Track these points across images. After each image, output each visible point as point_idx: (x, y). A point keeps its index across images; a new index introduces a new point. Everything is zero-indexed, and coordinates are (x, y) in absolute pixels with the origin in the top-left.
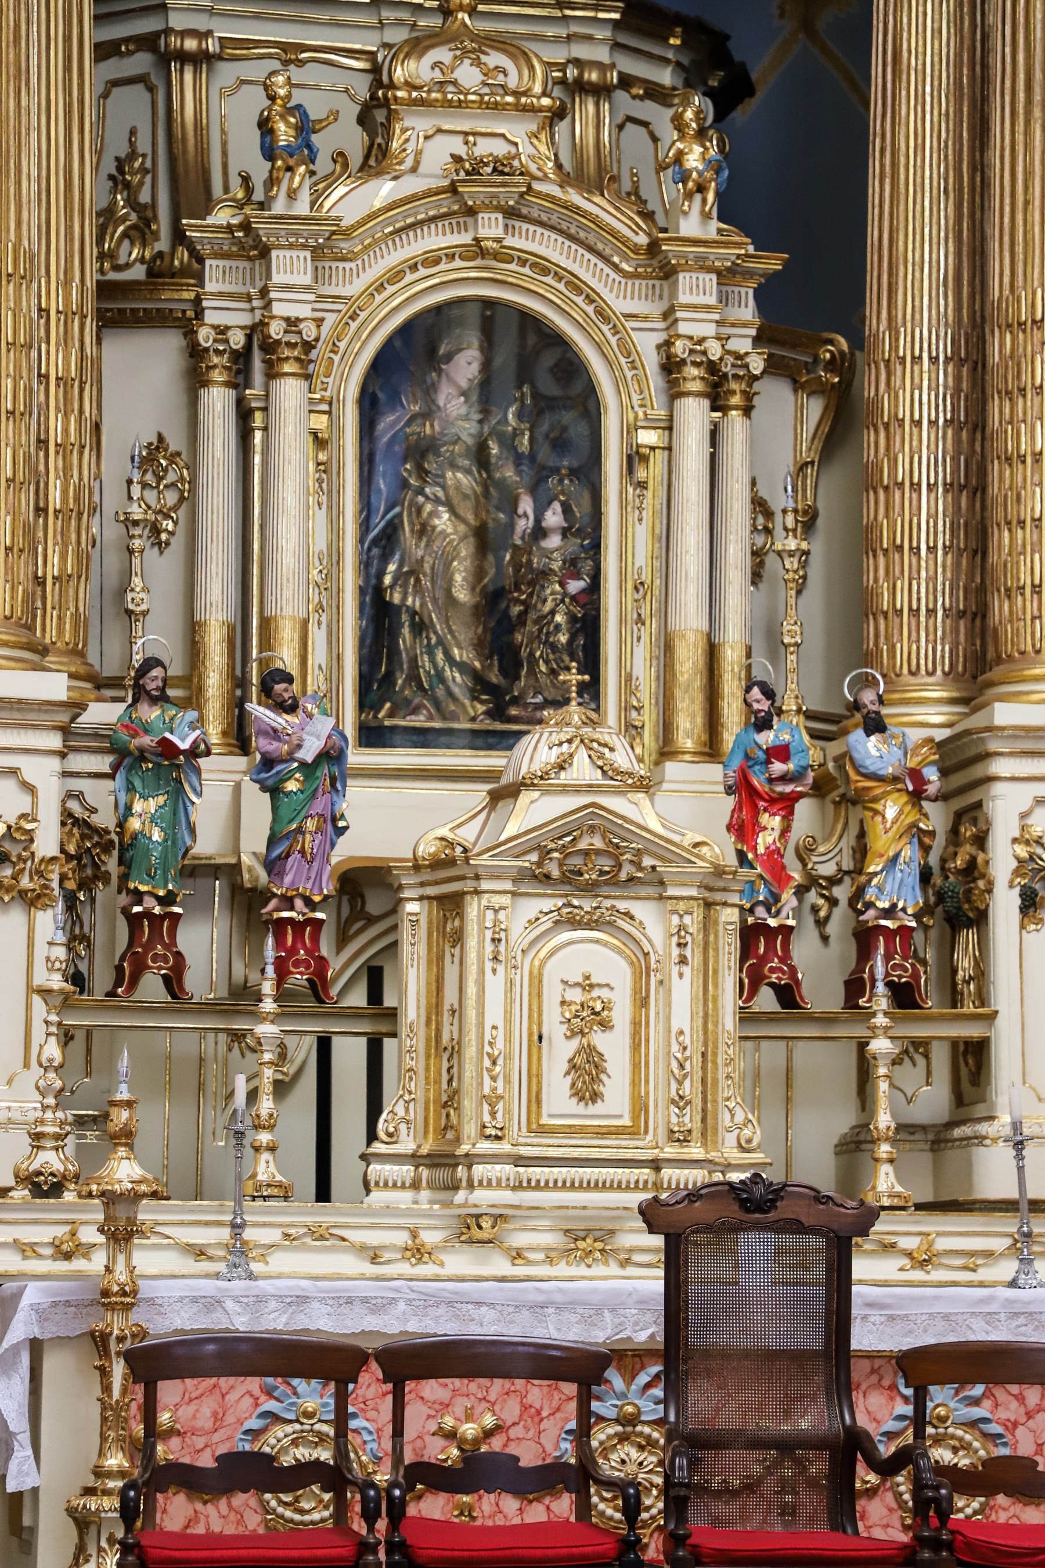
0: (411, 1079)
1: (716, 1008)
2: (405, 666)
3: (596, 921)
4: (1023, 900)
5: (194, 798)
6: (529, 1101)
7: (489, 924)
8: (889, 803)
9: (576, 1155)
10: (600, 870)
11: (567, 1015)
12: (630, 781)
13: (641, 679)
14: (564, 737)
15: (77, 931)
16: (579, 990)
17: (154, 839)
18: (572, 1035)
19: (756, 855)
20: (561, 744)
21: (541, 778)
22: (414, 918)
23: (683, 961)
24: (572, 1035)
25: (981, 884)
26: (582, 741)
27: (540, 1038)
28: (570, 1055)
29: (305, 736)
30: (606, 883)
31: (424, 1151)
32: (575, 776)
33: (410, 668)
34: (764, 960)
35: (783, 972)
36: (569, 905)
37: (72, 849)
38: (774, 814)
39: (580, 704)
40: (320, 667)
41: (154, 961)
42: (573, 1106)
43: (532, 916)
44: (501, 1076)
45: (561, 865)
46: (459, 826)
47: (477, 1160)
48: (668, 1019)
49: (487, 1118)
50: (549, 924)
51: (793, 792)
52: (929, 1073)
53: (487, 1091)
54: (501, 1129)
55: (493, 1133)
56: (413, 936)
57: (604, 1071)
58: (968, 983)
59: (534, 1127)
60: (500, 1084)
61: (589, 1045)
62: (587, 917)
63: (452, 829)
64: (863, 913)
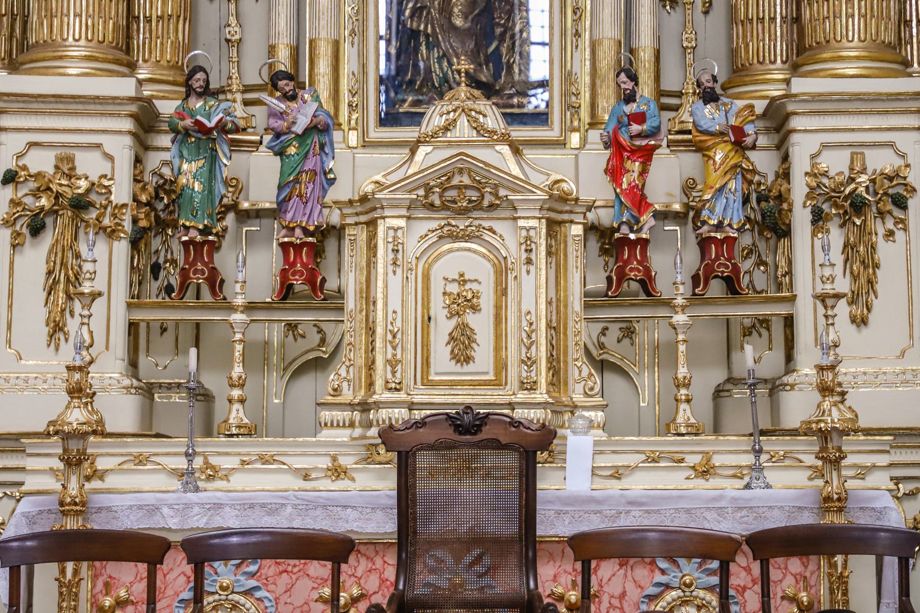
0: (350, 350)
1: (566, 297)
2: (422, 72)
3: (468, 236)
4: (813, 216)
5: (225, 161)
6: (422, 364)
7: (390, 240)
8: (718, 151)
9: (455, 401)
10: (469, 200)
11: (447, 302)
12: (495, 137)
13: (579, 75)
14: (450, 108)
15: (169, 257)
17: (196, 189)
18: (451, 316)
19: (622, 190)
20: (448, 113)
21: (433, 137)
22: (353, 238)
23: (529, 261)
24: (451, 316)
25: (785, 206)
26: (463, 110)
27: (429, 319)
28: (450, 331)
29: (299, 116)
30: (475, 208)
31: (357, 401)
32: (458, 135)
33: (425, 73)
35: (639, 271)
36: (449, 224)
37: (144, 198)
38: (635, 161)
39: (467, 85)
40: (353, 74)
41: (194, 274)
42: (452, 366)
43: (423, 233)
44: (400, 345)
45: (441, 196)
46: (389, 174)
48: (520, 303)
49: (389, 376)
50: (435, 239)
51: (647, 144)
52: (770, 341)
53: (389, 356)
54: (400, 383)
55: (393, 385)
56: (352, 250)
57: (475, 341)
58: (785, 276)
59: (425, 381)
61: (463, 323)
62: (462, 233)
63: (384, 176)
64: (701, 228)
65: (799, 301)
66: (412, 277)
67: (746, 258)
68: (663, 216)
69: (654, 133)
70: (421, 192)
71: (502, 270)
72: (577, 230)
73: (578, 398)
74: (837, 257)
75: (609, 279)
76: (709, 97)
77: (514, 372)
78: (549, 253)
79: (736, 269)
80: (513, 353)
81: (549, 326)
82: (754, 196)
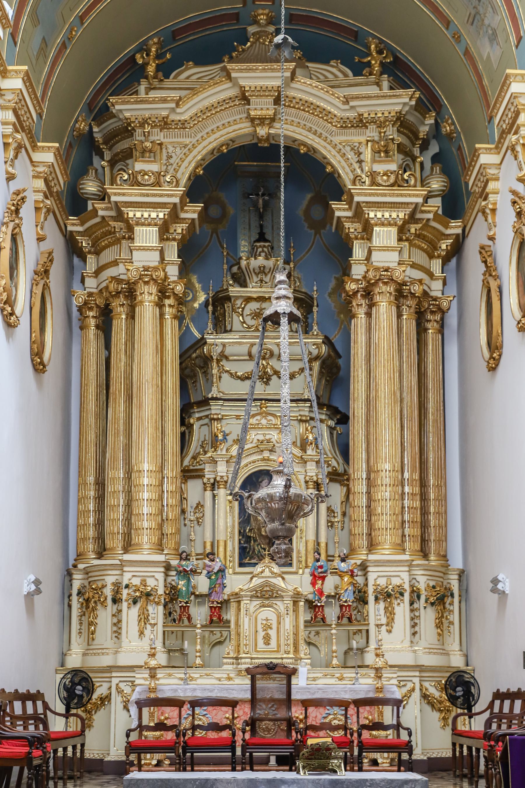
18: (264, 631)
34: (317, 612)
42: (264, 646)
65: (370, 625)
67: (354, 610)
68: (328, 597)
69: (326, 572)
71: (279, 616)
72: (302, 603)
73: (302, 656)
74: (382, 612)
75: (312, 617)
76: (343, 560)
77: (282, 648)
78: (294, 611)
79: (351, 615)
80: (282, 642)
81: (294, 634)
82: (357, 591)
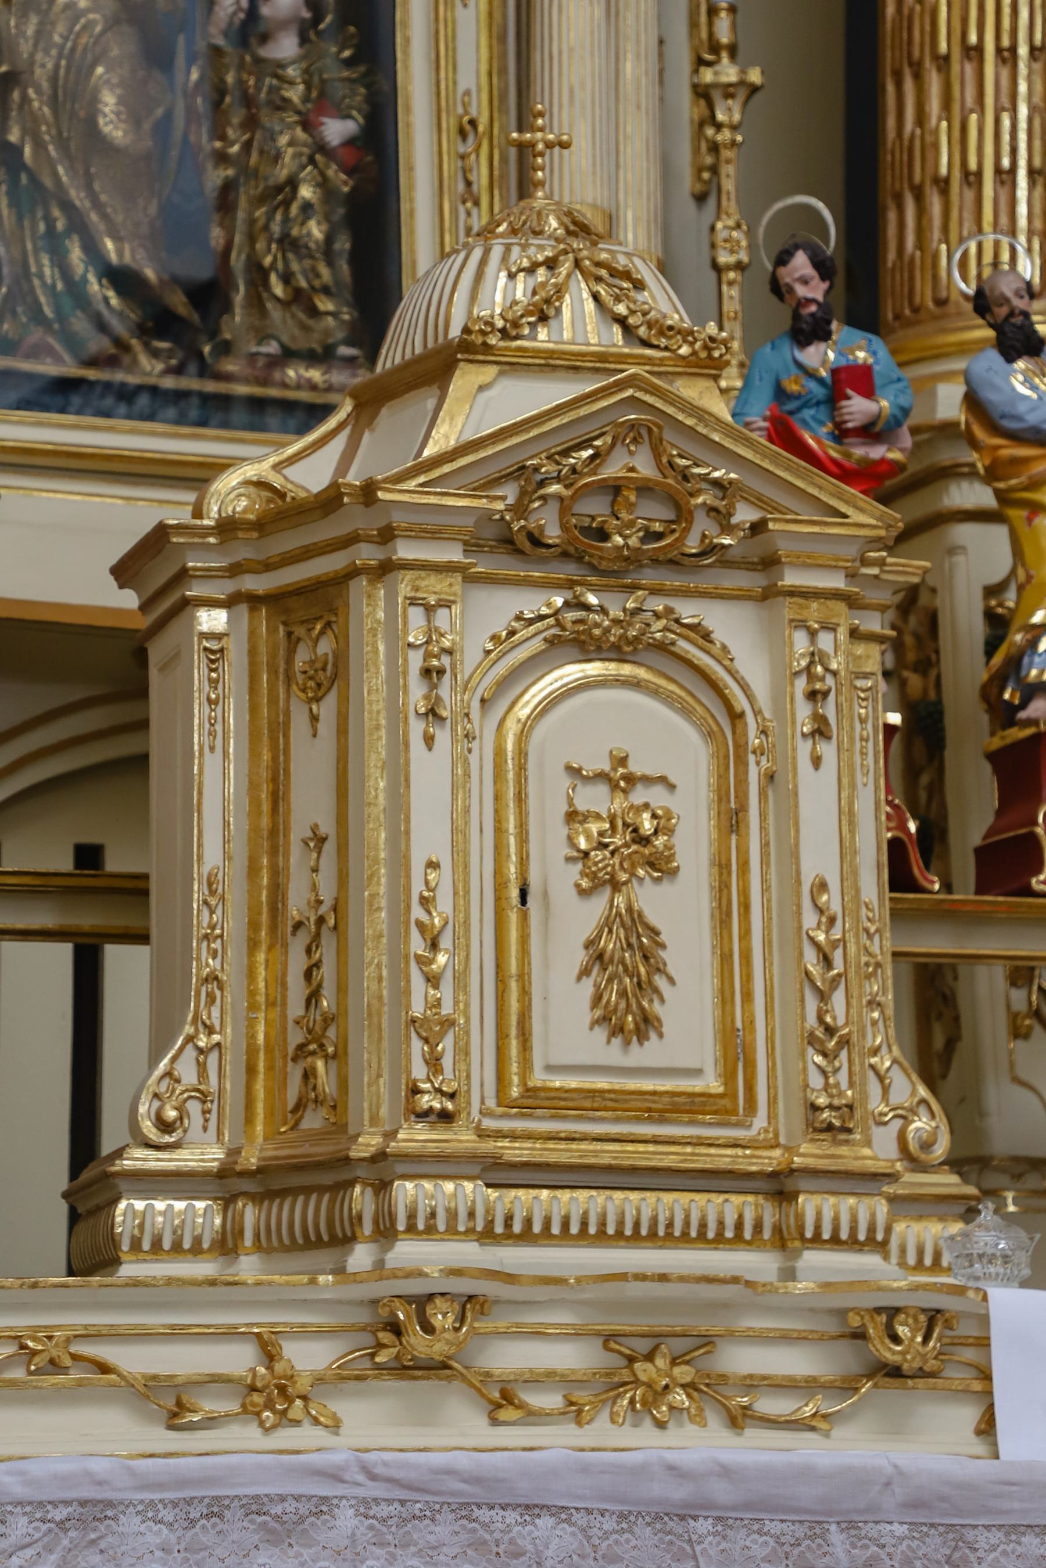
10: (646, 529)
16: (602, 790)
28: (588, 931)
47: (400, 1169)
48: (795, 855)
49: (419, 1071)
50: (536, 645)
57: (660, 969)
60: (446, 992)
61: (630, 909)
62: (617, 631)
66: (474, 759)
70: (510, 492)
